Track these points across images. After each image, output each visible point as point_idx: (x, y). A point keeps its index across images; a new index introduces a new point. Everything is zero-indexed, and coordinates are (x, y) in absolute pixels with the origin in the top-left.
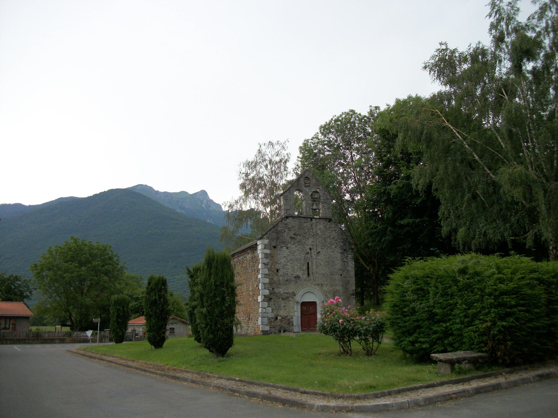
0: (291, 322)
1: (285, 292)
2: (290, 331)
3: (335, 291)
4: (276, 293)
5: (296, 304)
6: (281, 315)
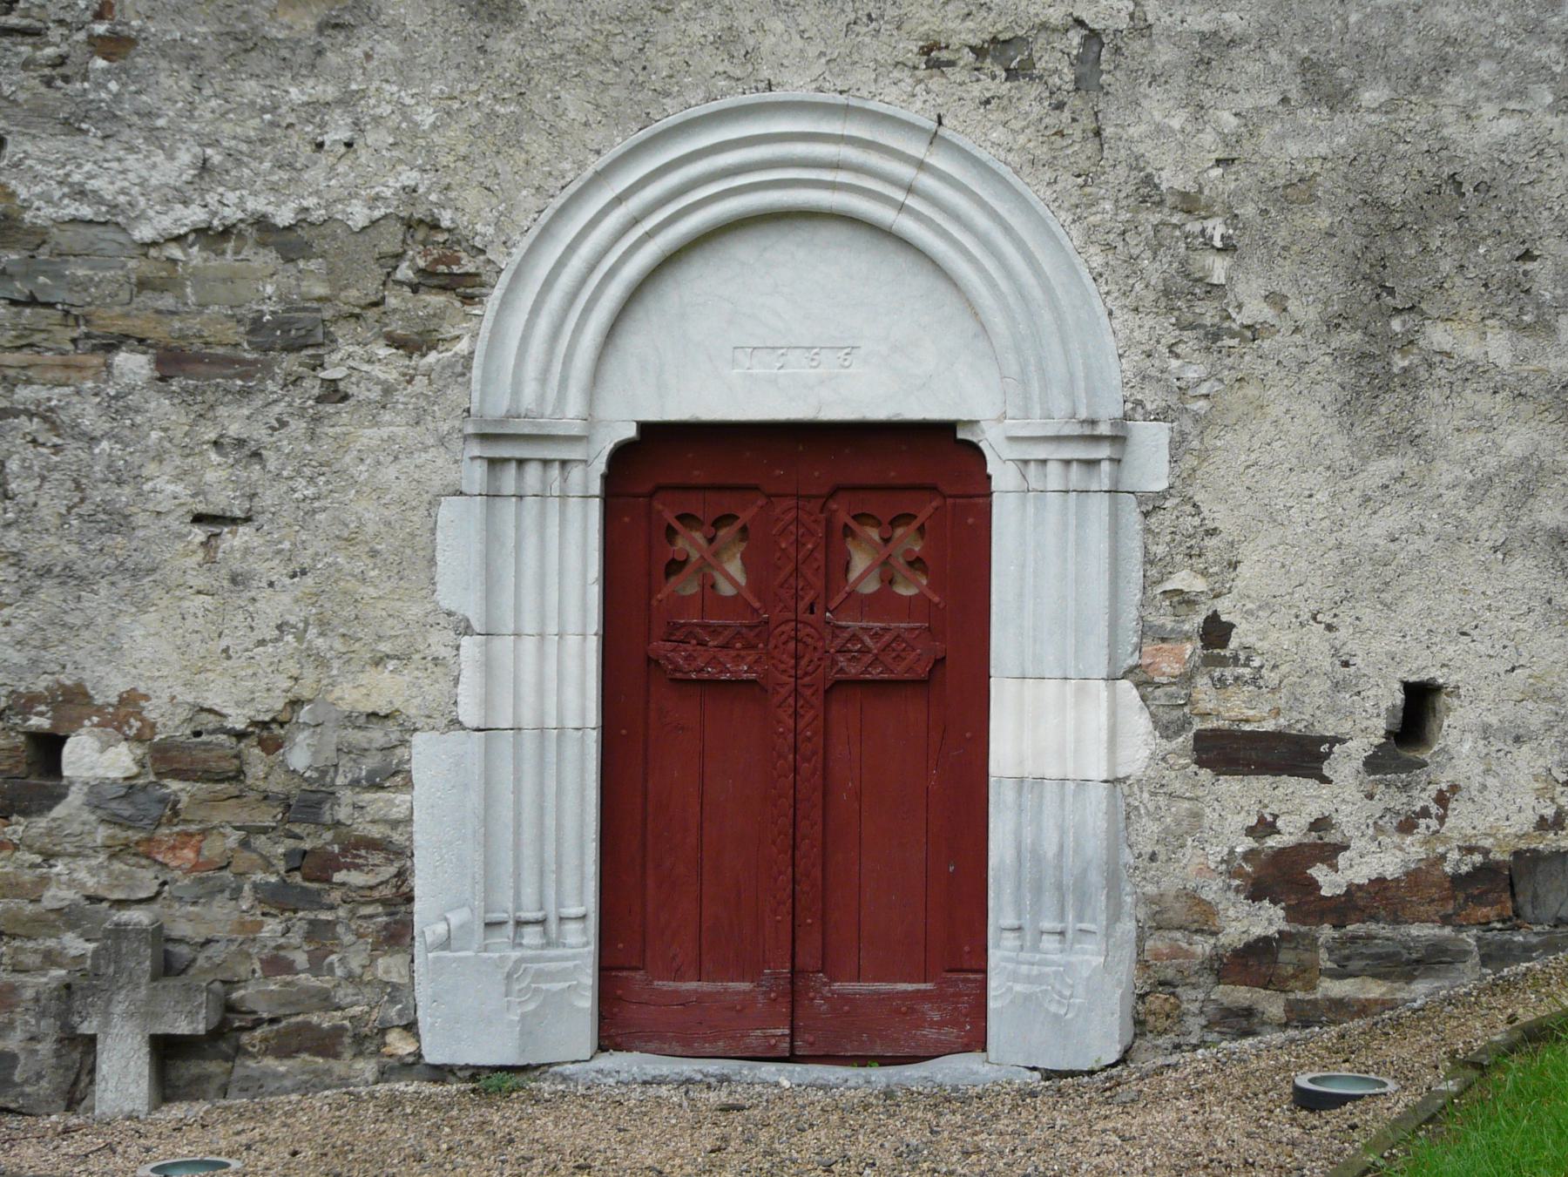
0: (358, 847)
1: (231, 205)
2: (326, 1044)
3: (1393, 187)
4: (38, 237)
5: (476, 476)
6: (131, 701)
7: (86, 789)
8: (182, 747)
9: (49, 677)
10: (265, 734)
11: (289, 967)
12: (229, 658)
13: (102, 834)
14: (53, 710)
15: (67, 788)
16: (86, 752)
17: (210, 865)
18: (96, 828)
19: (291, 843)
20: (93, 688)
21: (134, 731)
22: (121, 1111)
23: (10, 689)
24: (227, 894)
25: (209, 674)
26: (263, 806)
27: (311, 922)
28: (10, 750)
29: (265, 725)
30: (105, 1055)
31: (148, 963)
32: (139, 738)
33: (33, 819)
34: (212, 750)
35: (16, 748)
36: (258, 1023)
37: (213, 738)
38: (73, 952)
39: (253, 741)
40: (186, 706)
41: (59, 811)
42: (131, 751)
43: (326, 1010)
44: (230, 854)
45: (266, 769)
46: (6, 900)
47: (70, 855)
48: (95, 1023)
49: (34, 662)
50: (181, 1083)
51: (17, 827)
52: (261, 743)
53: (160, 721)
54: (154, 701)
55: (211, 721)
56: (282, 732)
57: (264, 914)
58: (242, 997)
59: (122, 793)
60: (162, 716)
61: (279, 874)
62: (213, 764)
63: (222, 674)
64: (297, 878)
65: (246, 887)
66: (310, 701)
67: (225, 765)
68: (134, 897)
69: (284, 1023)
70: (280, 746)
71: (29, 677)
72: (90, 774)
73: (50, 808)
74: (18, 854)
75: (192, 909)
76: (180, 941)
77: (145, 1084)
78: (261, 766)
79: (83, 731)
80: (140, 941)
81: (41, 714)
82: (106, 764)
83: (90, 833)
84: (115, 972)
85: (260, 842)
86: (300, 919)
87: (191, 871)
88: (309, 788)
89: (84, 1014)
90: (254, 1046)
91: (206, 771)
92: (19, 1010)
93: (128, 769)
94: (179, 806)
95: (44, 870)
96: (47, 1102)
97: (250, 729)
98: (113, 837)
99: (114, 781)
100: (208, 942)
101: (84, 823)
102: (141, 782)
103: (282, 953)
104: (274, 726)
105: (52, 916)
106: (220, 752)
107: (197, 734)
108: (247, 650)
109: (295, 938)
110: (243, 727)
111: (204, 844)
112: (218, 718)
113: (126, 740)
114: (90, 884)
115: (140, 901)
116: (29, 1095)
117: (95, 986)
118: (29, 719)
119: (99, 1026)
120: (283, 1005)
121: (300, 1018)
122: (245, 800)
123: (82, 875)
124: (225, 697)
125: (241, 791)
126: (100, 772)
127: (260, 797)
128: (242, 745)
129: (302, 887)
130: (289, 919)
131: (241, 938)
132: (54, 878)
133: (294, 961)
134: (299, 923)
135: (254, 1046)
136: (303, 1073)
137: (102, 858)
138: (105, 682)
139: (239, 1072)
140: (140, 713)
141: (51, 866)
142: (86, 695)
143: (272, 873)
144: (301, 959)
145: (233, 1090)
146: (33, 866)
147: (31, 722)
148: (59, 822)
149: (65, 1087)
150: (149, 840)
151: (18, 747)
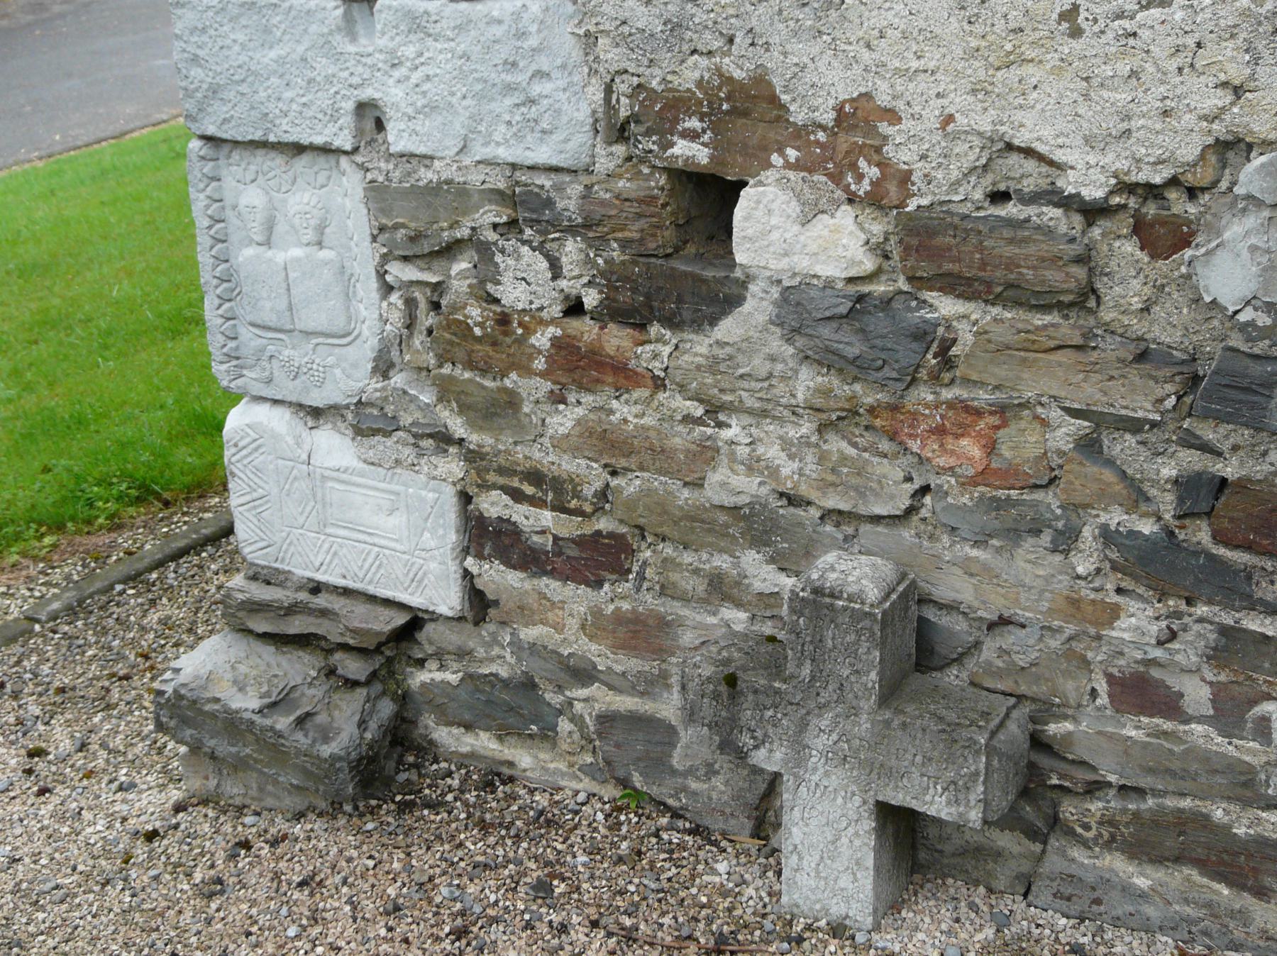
7: (775, 292)
8: (962, 226)
9: (704, 62)
10: (1151, 210)
11: (1170, 705)
12: (1076, 33)
13: (807, 382)
14: (715, 128)
15: (743, 285)
16: (774, 221)
17: (1009, 475)
18: (796, 372)
19: (1192, 460)
20: (786, 89)
21: (866, 186)
22: (827, 912)
23: (635, 80)
24: (1046, 538)
25: (1029, 69)
26: (1133, 373)
27: (1224, 631)
28: (640, 201)
29: (1151, 191)
30: (797, 813)
31: (873, 675)
32: (875, 201)
33: (686, 336)
34: (1025, 241)
35: (649, 200)
36: (1094, 788)
37: (1031, 211)
38: (758, 586)
39: (1124, 224)
40: (977, 142)
41: (728, 328)
42: (861, 226)
43: (1246, 803)
44: (1057, 461)
45: (1147, 290)
46: (646, 475)
47: (750, 412)
48: (778, 755)
49: (675, 27)
50: (948, 848)
51: (660, 347)
52: (1140, 229)
53: (919, 169)
54: (907, 124)
55: (1031, 176)
56: (1192, 209)
57: (1119, 591)
58: (1070, 734)
59: (843, 310)
60: (923, 157)
61: (1159, 519)
62: (1029, 274)
63: (1057, 71)
64: (1201, 534)
65: (1087, 532)
66: (1267, 145)
67: (1053, 276)
68: (863, 510)
69: (1151, 802)
70: (1185, 242)
71: (665, 57)
72: (784, 263)
73: (713, 321)
74: (661, 396)
75: (975, 553)
76: (951, 607)
77: (866, 881)
78: (1136, 284)
79: (769, 175)
80: (859, 633)
81: (693, 136)
82: (813, 247)
83: (784, 378)
84: (813, 678)
85: (1123, 446)
86: (1201, 620)
87: (973, 482)
88: (1244, 348)
89: (759, 734)
90: (1087, 827)
91: (1010, 286)
92: (674, 660)
93: (853, 263)
94: (954, 351)
95: (709, 431)
96: (723, 813)
97: (1116, 200)
98: (826, 392)
99: (829, 284)
100: (1003, 622)
101: (772, 359)
102: (879, 288)
103: (1155, 673)
104: (1172, 195)
105: (723, 518)
106: (1045, 248)
107: (999, 197)
108: (1120, 16)
109: (1187, 652)
110: (1099, 194)
111: (1001, 433)
112: (1045, 169)
113: (850, 201)
114: (785, 471)
115: (876, 519)
116: (695, 793)
117: (777, 692)
118: (672, 145)
119: (785, 762)
120: (1151, 771)
121: (1186, 803)
122: (1094, 355)
123: (773, 452)
124: (1061, 125)
125: (1088, 335)
126: (803, 264)
127: (1128, 354)
128: (1096, 232)
129: (1212, 558)
130: (1178, 615)
131: (1070, 629)
132: (725, 450)
133: (1182, 695)
134: (1197, 627)
135: (1087, 827)
136: (1187, 901)
137: (806, 428)
138: (809, 77)
139: (1053, 863)
140: (878, 150)
141: (720, 425)
142: (774, 100)
143: (1144, 515)
144: (1197, 694)
145: (1042, 893)
146: (688, 419)
147: (676, 150)
148: (728, 350)
149: (752, 798)
150: (895, 408)
151: (655, 198)
